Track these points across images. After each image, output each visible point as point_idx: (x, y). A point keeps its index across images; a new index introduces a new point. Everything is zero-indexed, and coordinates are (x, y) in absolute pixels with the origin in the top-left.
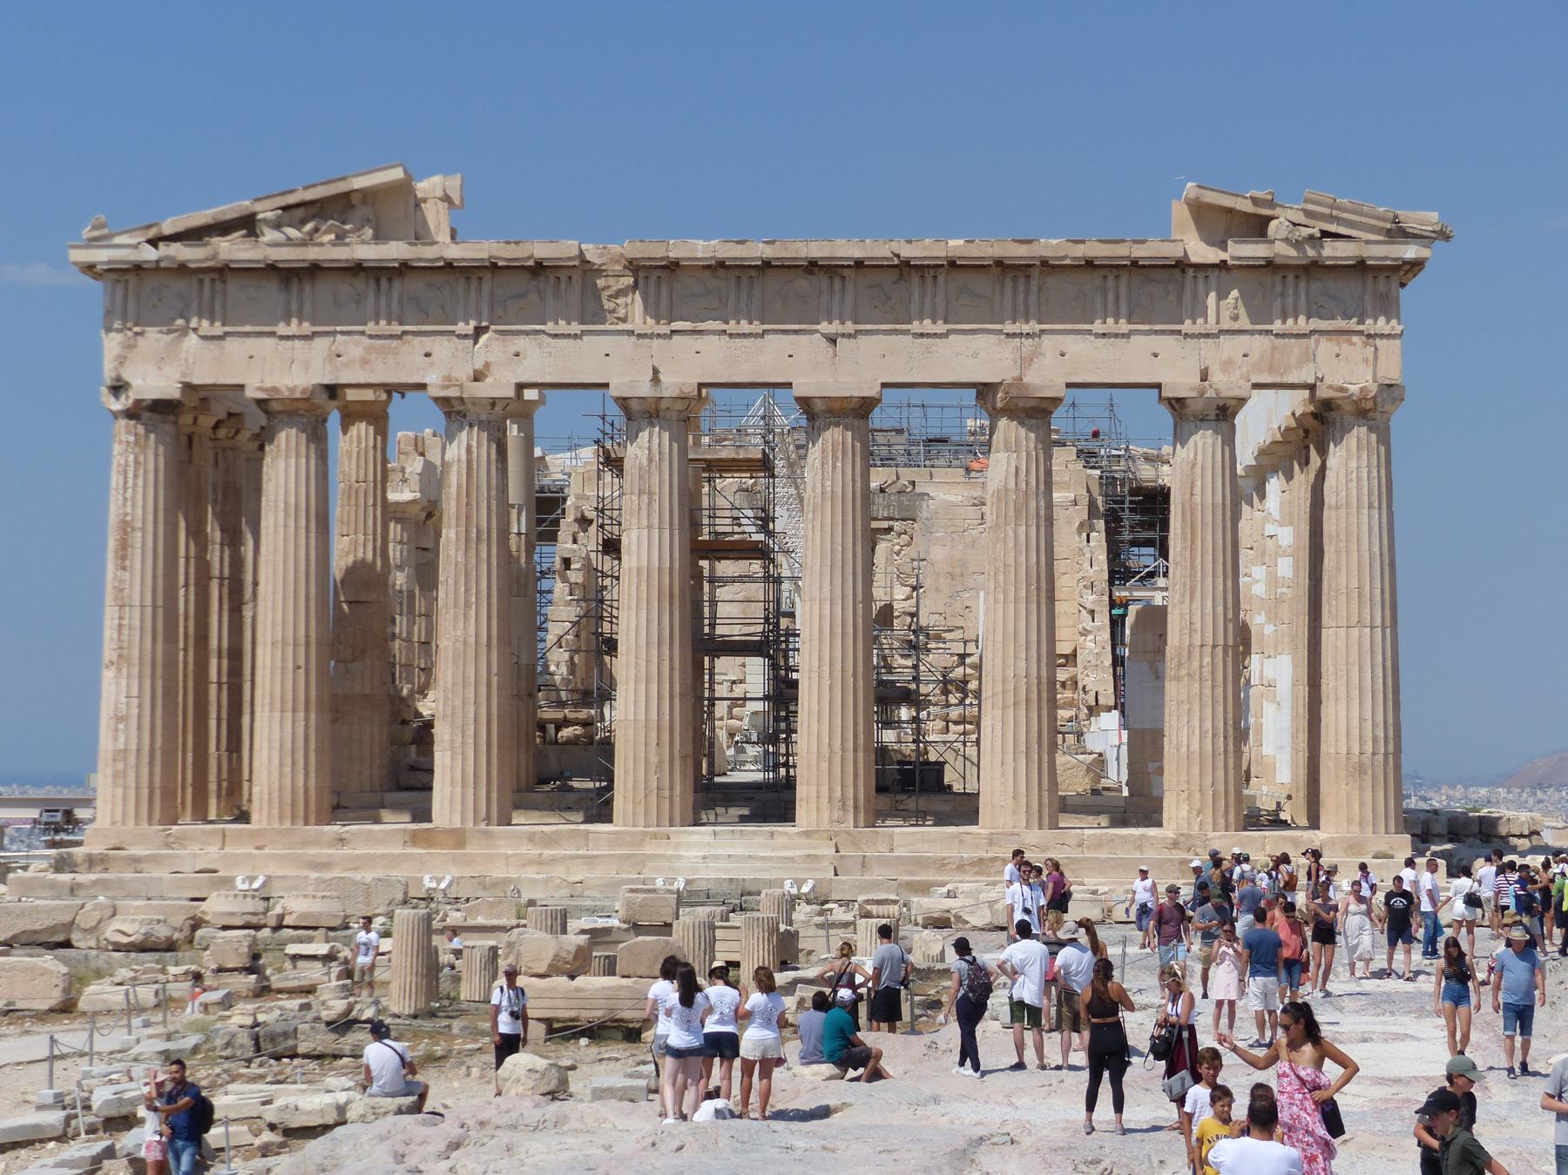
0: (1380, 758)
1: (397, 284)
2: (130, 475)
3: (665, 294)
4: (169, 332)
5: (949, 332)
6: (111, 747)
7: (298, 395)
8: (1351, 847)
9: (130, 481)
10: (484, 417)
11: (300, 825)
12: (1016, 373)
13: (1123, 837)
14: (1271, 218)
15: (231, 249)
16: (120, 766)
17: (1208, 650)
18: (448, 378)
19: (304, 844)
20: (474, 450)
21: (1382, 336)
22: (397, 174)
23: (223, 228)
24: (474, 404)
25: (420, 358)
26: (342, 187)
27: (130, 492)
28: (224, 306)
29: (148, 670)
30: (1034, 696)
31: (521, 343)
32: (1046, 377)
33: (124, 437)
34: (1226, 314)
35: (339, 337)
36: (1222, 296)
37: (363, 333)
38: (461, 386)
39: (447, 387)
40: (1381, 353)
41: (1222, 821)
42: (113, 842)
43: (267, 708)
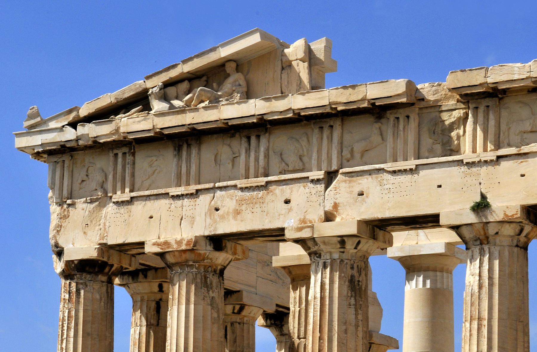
1: (264, 141)
3: (492, 122)
4: (92, 202)
7: (184, 247)
10: (336, 256)
18: (303, 221)
20: (327, 287)
22: (255, 39)
24: (324, 243)
28: (133, 175)
31: (365, 182)
35: (219, 193)
39: (300, 229)
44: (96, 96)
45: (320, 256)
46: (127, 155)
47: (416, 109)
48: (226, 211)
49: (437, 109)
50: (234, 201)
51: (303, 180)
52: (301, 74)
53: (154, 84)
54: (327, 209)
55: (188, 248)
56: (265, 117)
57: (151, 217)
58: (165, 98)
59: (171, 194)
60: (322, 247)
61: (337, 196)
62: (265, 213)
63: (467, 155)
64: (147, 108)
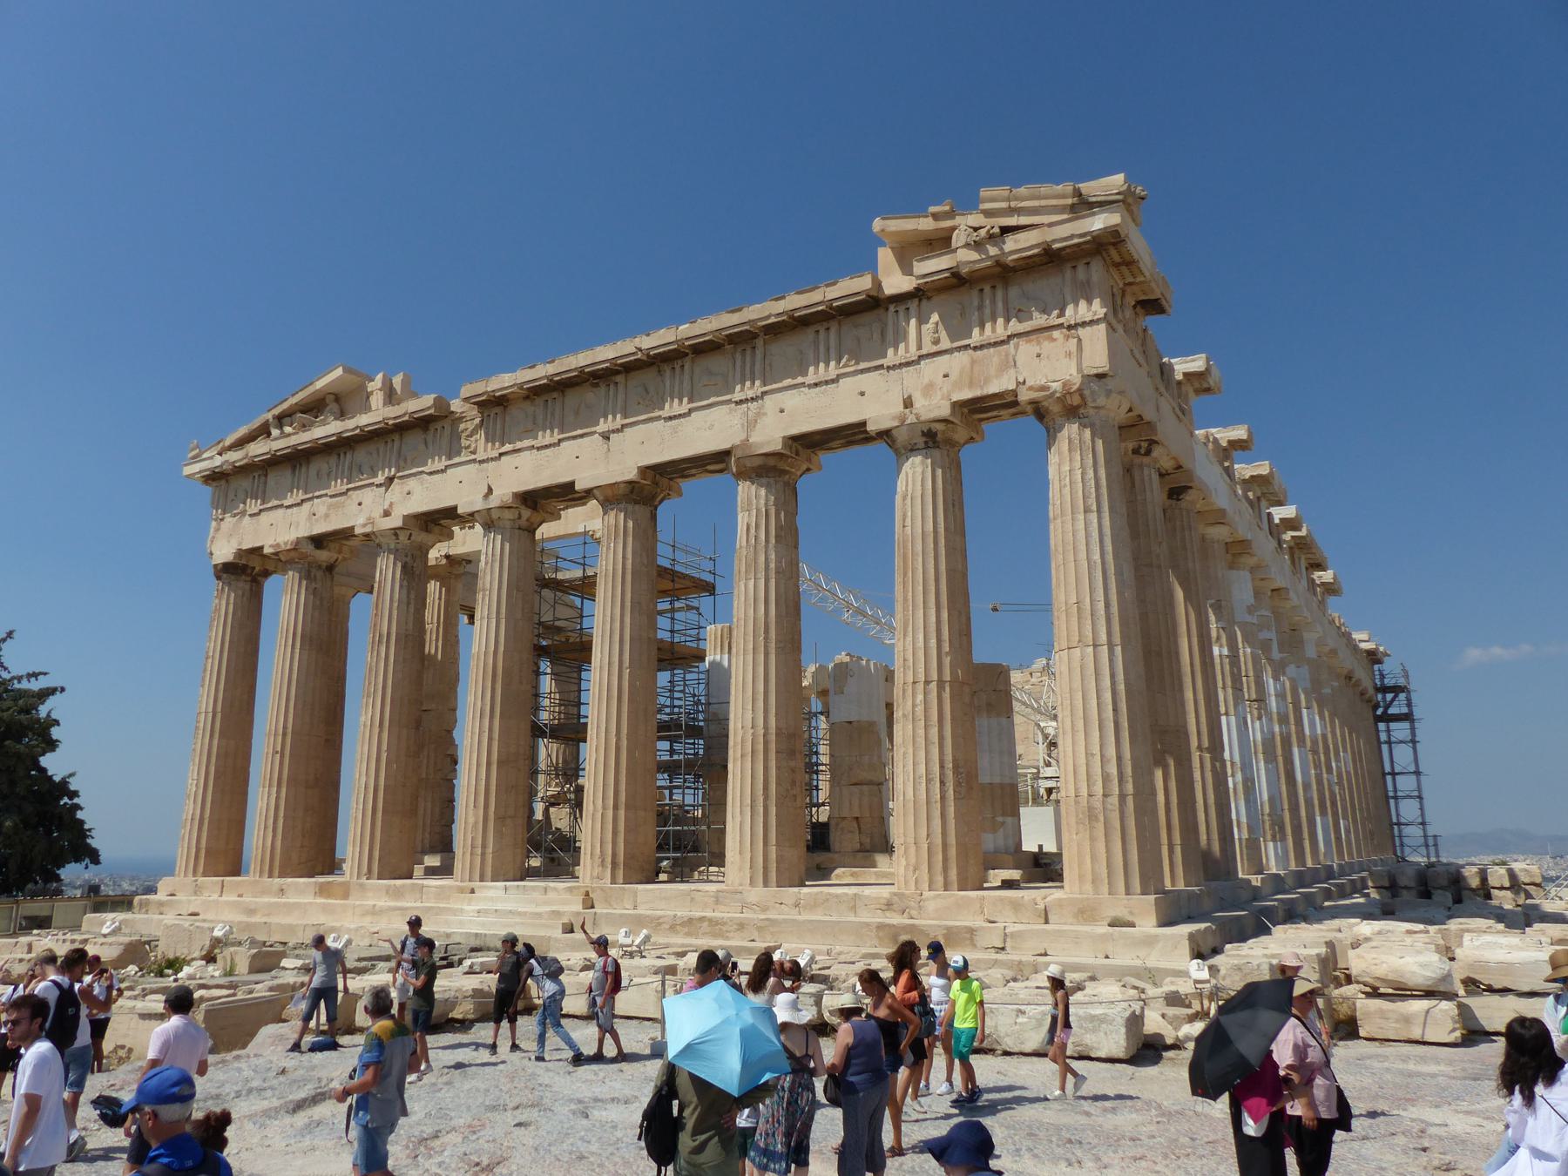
0: (1114, 800)
1: (349, 456)
5: (690, 411)
8: (1081, 912)
11: (266, 879)
12: (743, 436)
13: (837, 896)
14: (953, 229)
17: (920, 687)
21: (1084, 324)
22: (339, 372)
25: (355, 507)
26: (310, 390)
30: (761, 747)
31: (412, 483)
32: (770, 434)
34: (927, 340)
36: (922, 321)
40: (1085, 343)
41: (940, 879)
44: (234, 430)
47: (448, 421)
53: (269, 416)
58: (281, 427)
63: (480, 456)
64: (269, 434)
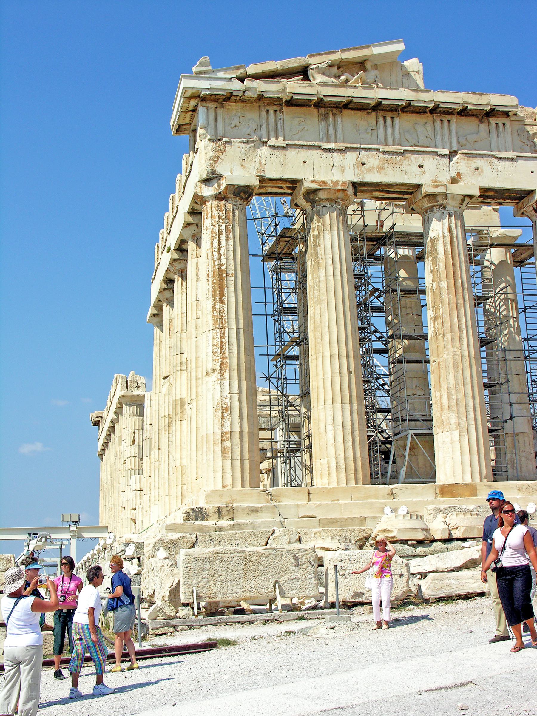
1: (397, 121)
2: (223, 237)
4: (248, 143)
6: (218, 432)
7: (339, 187)
9: (223, 243)
15: (294, 87)
16: (228, 444)
18: (435, 181)
19: (367, 498)
20: (454, 229)
23: (288, 74)
24: (453, 199)
27: (223, 251)
29: (243, 374)
31: (479, 162)
33: (216, 213)
35: (363, 153)
37: (378, 150)
38: (445, 186)
39: (437, 186)
42: (226, 499)
43: (330, 402)
45: (445, 208)
46: (278, 113)
48: (372, 166)
49: (522, 123)
50: (378, 160)
51: (432, 153)
52: (418, 82)
54: (453, 175)
55: (344, 188)
56: (413, 103)
57: (305, 162)
59: (323, 147)
60: (450, 201)
61: (459, 168)
62: (404, 172)
